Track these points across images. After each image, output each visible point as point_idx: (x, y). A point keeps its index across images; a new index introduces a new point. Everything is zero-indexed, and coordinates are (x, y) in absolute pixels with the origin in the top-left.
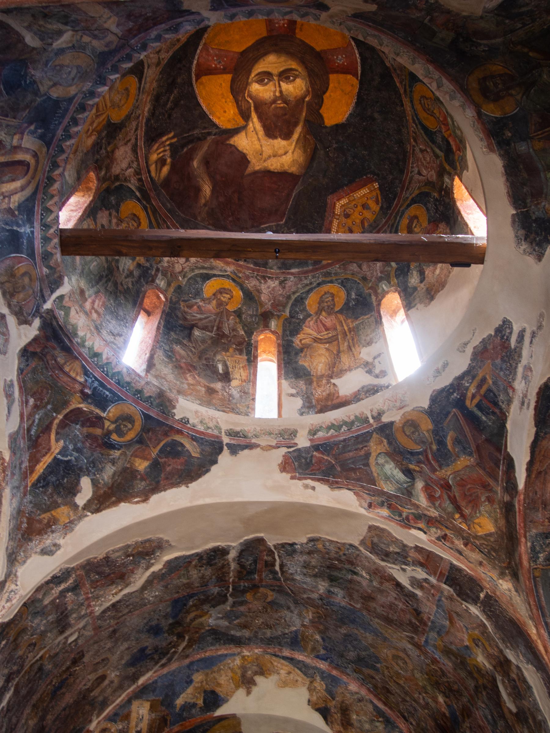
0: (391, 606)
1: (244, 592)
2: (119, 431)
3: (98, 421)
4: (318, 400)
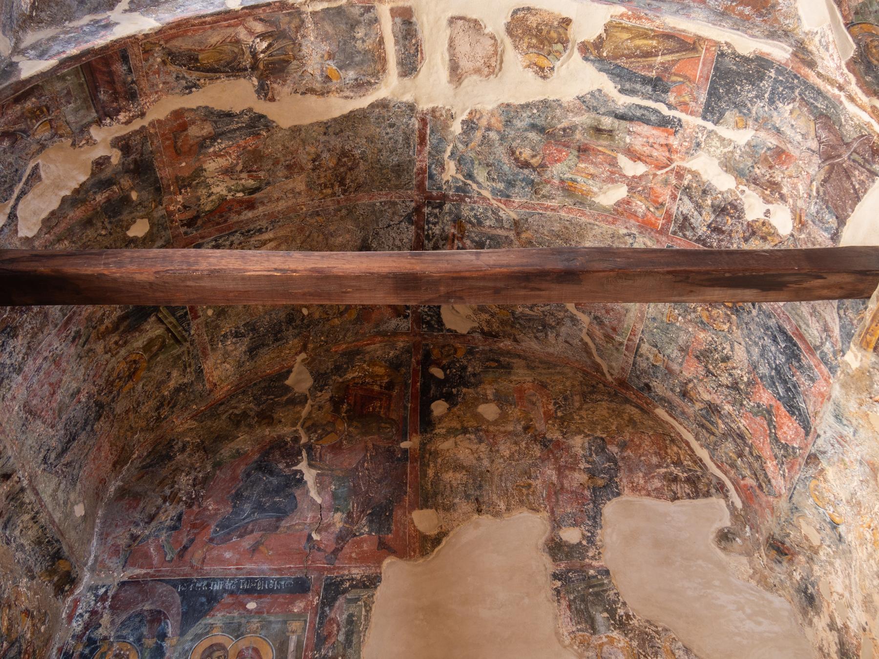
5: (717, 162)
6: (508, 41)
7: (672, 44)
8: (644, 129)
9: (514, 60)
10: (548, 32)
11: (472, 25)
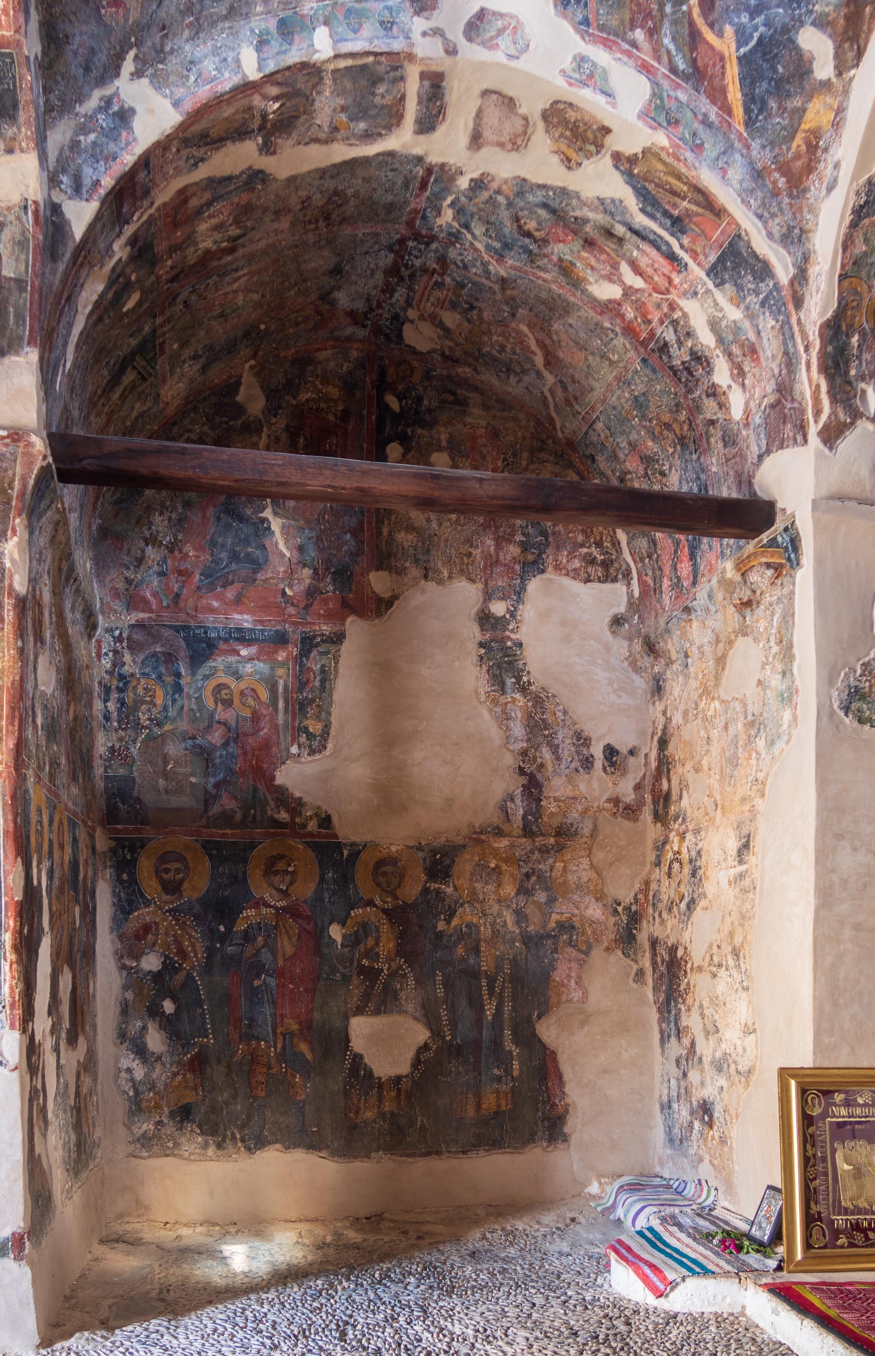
5: (706, 318)
8: (653, 253)
10: (585, 131)
11: (506, 101)
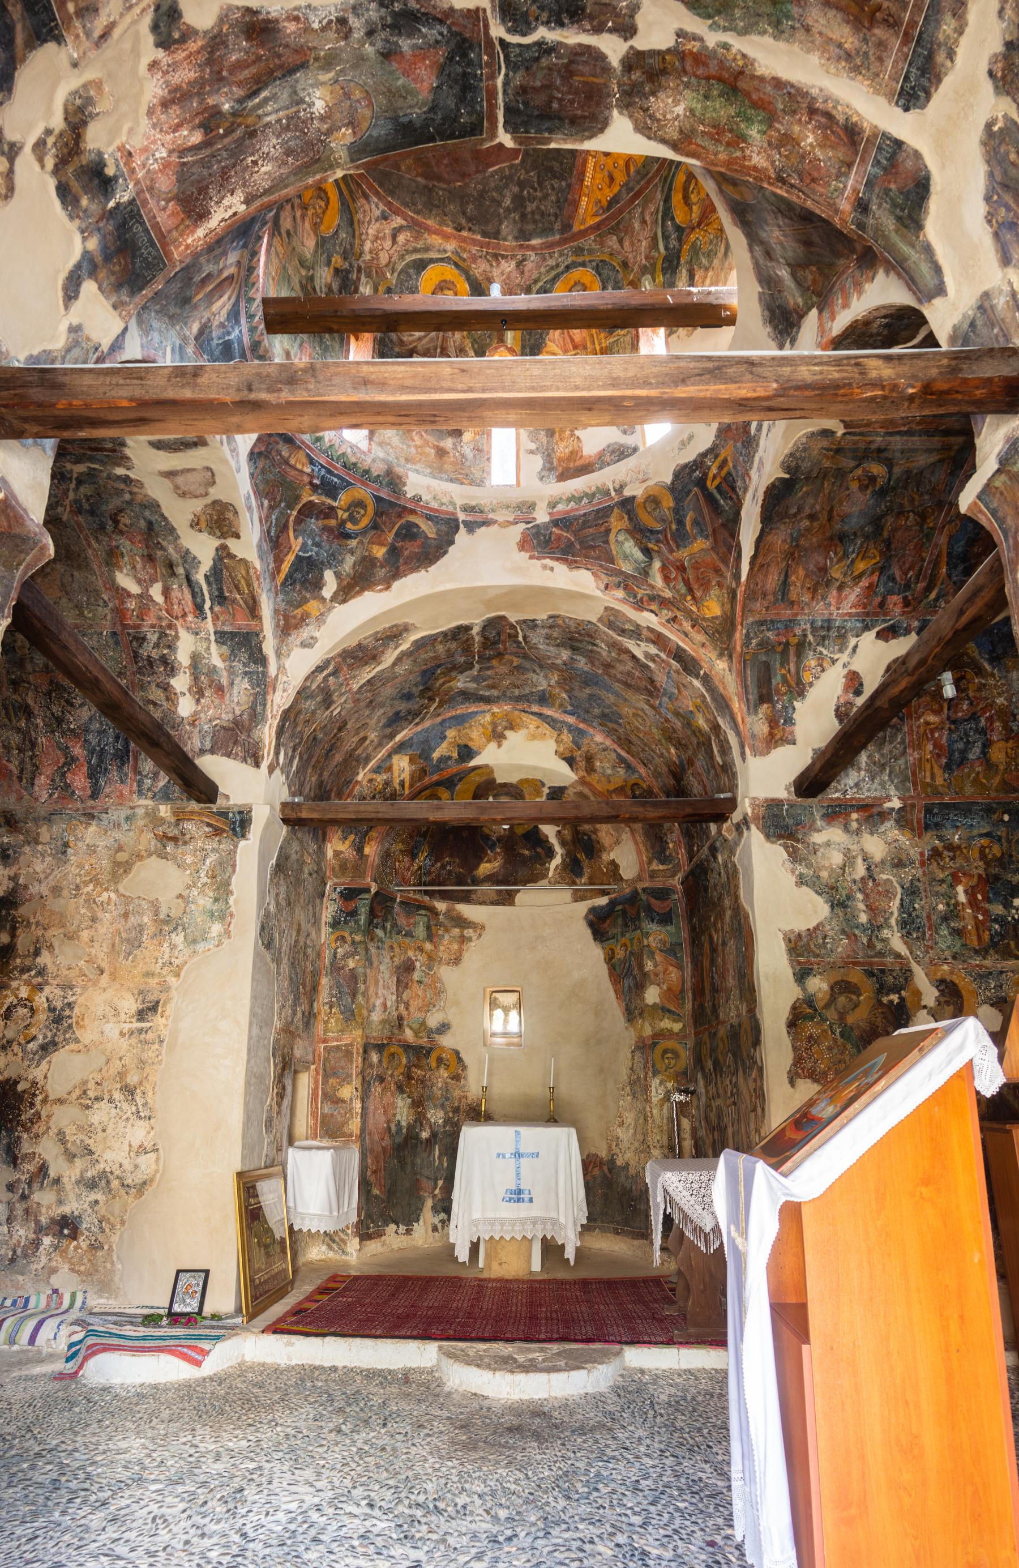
0: (629, 674)
1: (490, 659)
2: (352, 519)
3: (330, 512)
4: (560, 460)
6: (208, 500)
7: (251, 602)
9: (197, 506)
